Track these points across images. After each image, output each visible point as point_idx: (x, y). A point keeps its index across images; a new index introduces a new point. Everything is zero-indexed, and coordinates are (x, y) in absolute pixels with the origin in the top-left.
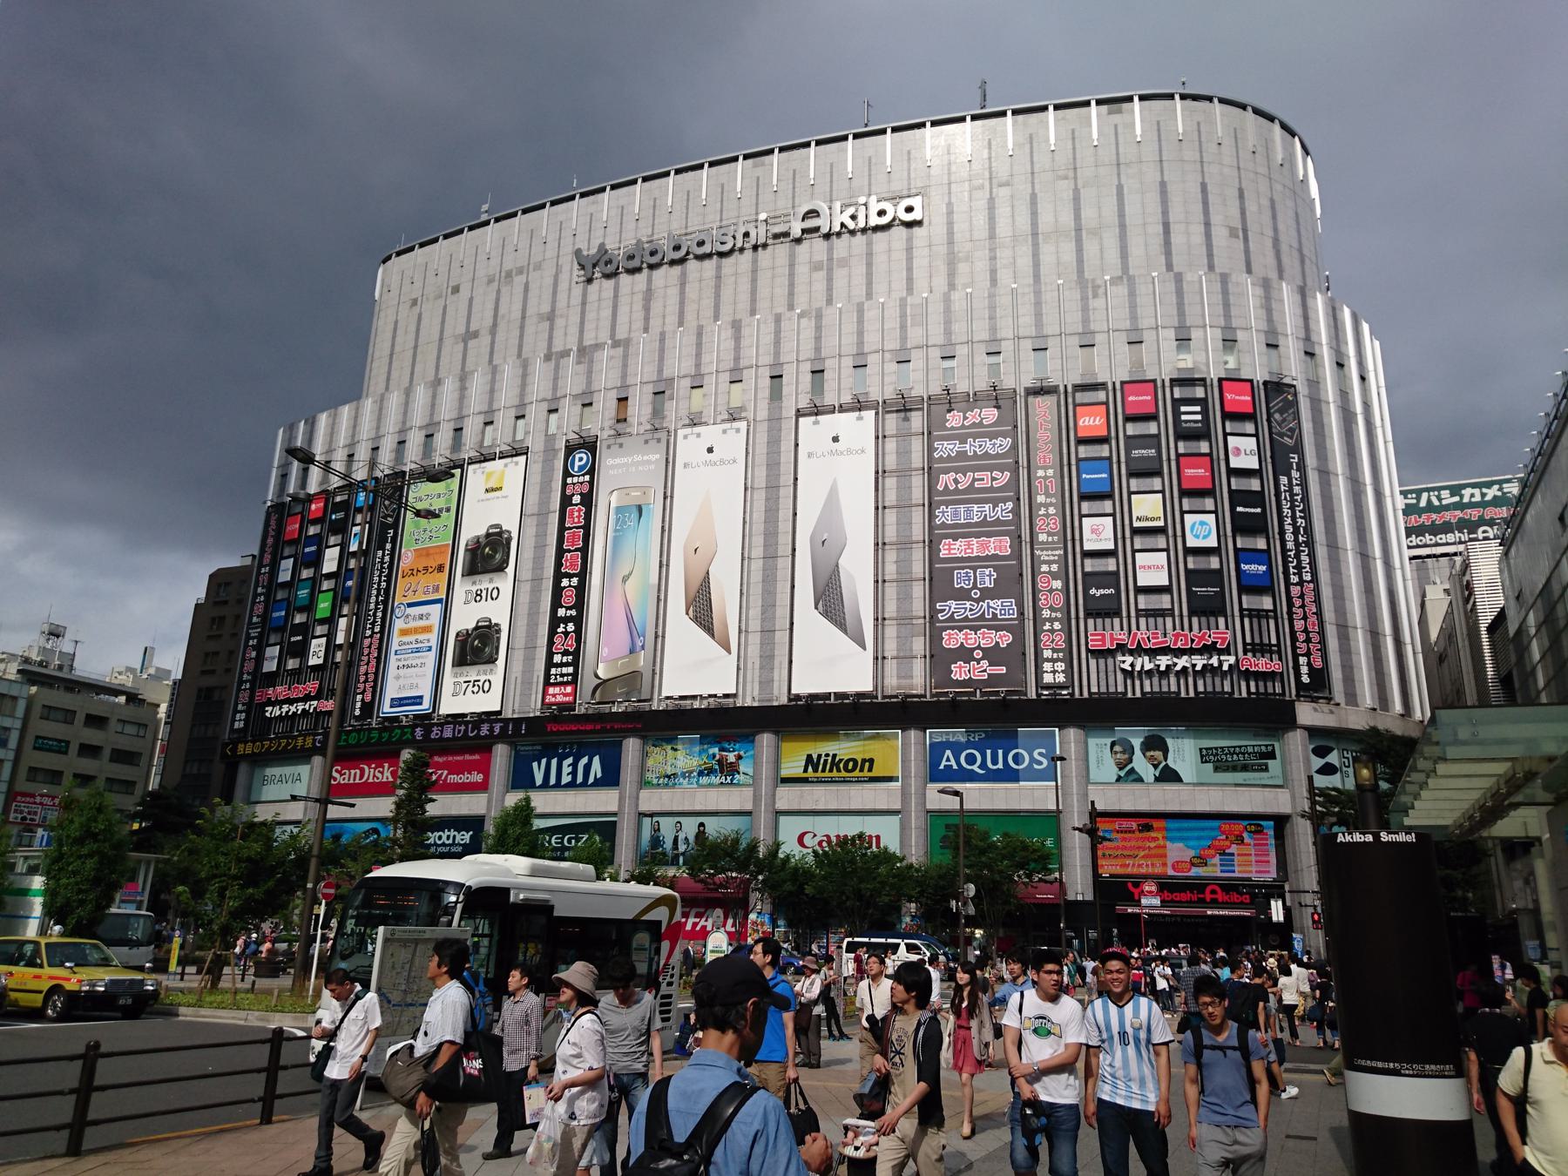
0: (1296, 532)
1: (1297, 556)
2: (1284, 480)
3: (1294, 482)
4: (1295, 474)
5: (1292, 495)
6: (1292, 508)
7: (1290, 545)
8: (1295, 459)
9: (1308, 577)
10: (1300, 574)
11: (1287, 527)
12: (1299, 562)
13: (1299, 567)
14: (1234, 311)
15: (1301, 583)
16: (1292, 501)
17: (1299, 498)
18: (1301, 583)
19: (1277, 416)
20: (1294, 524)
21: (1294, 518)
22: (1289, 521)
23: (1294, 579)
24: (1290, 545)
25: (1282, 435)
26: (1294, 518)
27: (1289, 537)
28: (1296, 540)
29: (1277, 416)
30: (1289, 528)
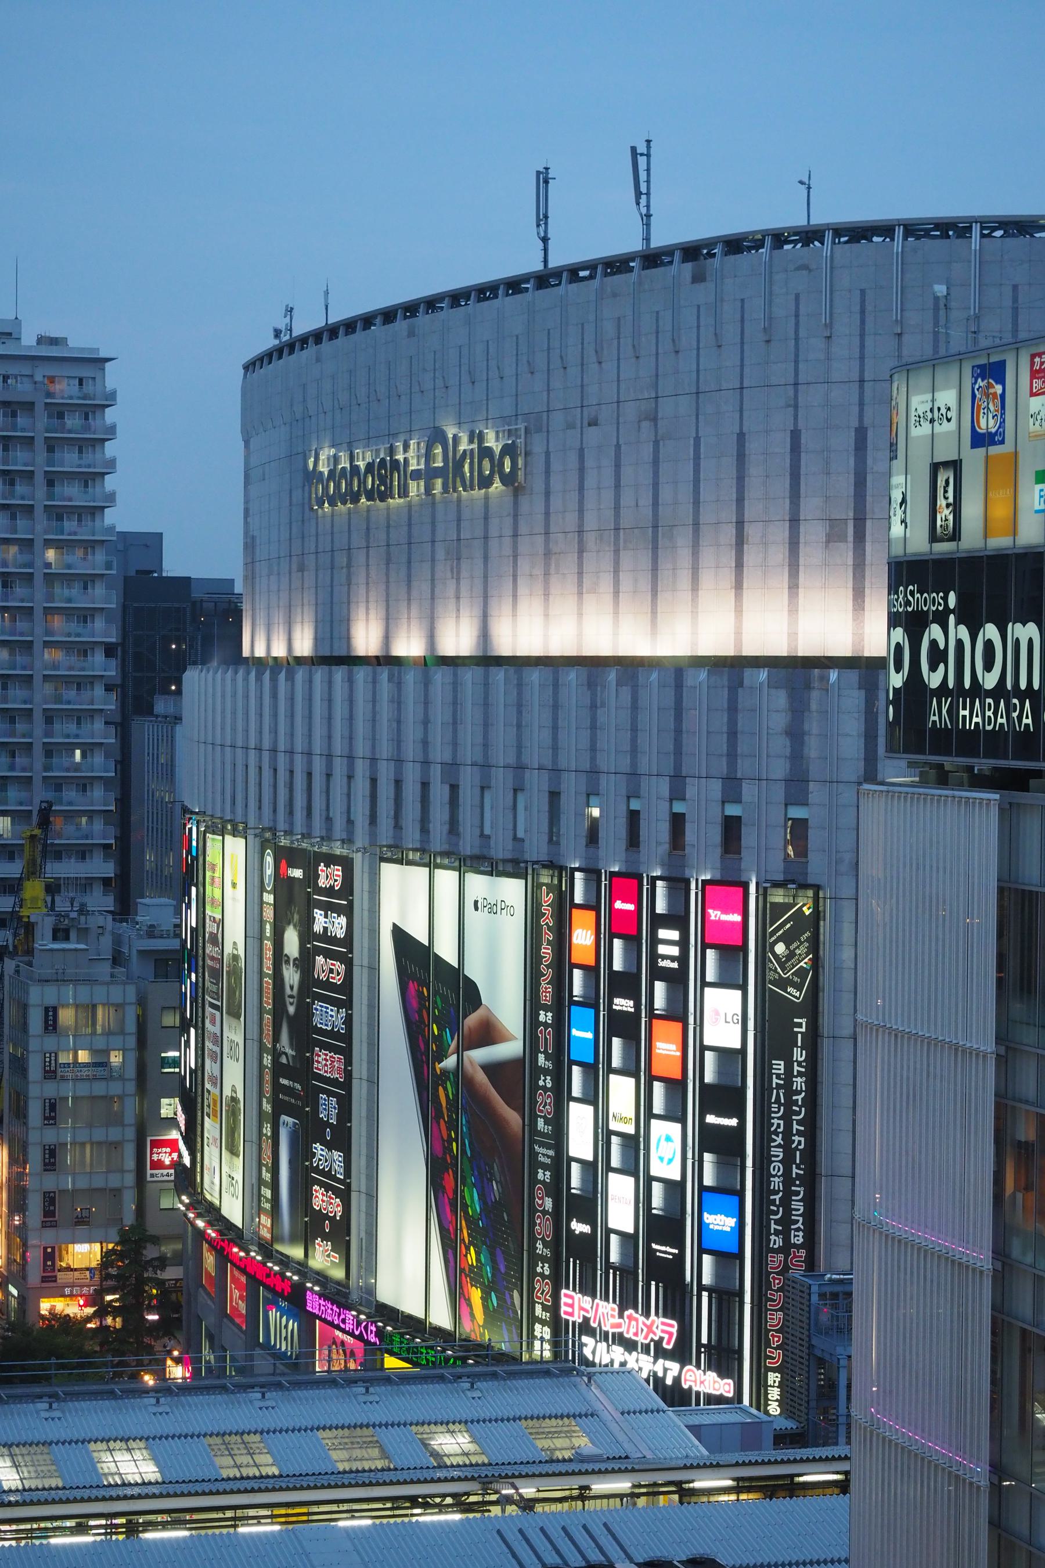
0: (788, 1161)
1: (786, 1202)
2: (779, 1066)
3: (796, 1068)
4: (799, 1055)
5: (790, 1092)
6: (787, 1118)
7: (776, 1183)
8: (801, 1027)
9: (798, 1238)
10: (785, 1234)
11: (774, 1151)
12: (788, 1211)
13: (786, 1222)
14: (743, 746)
15: (787, 1247)
16: (789, 1103)
17: (799, 1098)
18: (787, 1247)
19: (780, 948)
20: (787, 1146)
21: (788, 1134)
22: (779, 1140)
23: (776, 1241)
24: (776, 1183)
25: (783, 983)
26: (788, 1134)
27: (776, 1168)
28: (787, 1172)
29: (780, 948)
30: (778, 1153)
